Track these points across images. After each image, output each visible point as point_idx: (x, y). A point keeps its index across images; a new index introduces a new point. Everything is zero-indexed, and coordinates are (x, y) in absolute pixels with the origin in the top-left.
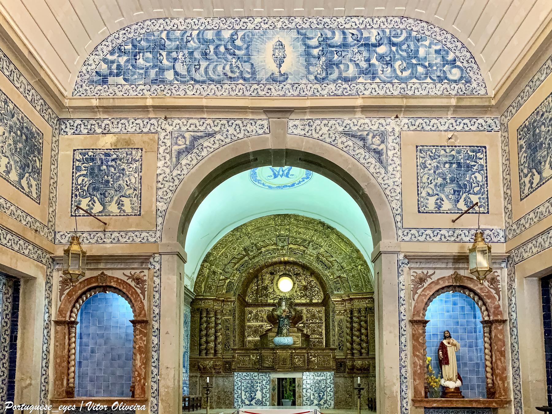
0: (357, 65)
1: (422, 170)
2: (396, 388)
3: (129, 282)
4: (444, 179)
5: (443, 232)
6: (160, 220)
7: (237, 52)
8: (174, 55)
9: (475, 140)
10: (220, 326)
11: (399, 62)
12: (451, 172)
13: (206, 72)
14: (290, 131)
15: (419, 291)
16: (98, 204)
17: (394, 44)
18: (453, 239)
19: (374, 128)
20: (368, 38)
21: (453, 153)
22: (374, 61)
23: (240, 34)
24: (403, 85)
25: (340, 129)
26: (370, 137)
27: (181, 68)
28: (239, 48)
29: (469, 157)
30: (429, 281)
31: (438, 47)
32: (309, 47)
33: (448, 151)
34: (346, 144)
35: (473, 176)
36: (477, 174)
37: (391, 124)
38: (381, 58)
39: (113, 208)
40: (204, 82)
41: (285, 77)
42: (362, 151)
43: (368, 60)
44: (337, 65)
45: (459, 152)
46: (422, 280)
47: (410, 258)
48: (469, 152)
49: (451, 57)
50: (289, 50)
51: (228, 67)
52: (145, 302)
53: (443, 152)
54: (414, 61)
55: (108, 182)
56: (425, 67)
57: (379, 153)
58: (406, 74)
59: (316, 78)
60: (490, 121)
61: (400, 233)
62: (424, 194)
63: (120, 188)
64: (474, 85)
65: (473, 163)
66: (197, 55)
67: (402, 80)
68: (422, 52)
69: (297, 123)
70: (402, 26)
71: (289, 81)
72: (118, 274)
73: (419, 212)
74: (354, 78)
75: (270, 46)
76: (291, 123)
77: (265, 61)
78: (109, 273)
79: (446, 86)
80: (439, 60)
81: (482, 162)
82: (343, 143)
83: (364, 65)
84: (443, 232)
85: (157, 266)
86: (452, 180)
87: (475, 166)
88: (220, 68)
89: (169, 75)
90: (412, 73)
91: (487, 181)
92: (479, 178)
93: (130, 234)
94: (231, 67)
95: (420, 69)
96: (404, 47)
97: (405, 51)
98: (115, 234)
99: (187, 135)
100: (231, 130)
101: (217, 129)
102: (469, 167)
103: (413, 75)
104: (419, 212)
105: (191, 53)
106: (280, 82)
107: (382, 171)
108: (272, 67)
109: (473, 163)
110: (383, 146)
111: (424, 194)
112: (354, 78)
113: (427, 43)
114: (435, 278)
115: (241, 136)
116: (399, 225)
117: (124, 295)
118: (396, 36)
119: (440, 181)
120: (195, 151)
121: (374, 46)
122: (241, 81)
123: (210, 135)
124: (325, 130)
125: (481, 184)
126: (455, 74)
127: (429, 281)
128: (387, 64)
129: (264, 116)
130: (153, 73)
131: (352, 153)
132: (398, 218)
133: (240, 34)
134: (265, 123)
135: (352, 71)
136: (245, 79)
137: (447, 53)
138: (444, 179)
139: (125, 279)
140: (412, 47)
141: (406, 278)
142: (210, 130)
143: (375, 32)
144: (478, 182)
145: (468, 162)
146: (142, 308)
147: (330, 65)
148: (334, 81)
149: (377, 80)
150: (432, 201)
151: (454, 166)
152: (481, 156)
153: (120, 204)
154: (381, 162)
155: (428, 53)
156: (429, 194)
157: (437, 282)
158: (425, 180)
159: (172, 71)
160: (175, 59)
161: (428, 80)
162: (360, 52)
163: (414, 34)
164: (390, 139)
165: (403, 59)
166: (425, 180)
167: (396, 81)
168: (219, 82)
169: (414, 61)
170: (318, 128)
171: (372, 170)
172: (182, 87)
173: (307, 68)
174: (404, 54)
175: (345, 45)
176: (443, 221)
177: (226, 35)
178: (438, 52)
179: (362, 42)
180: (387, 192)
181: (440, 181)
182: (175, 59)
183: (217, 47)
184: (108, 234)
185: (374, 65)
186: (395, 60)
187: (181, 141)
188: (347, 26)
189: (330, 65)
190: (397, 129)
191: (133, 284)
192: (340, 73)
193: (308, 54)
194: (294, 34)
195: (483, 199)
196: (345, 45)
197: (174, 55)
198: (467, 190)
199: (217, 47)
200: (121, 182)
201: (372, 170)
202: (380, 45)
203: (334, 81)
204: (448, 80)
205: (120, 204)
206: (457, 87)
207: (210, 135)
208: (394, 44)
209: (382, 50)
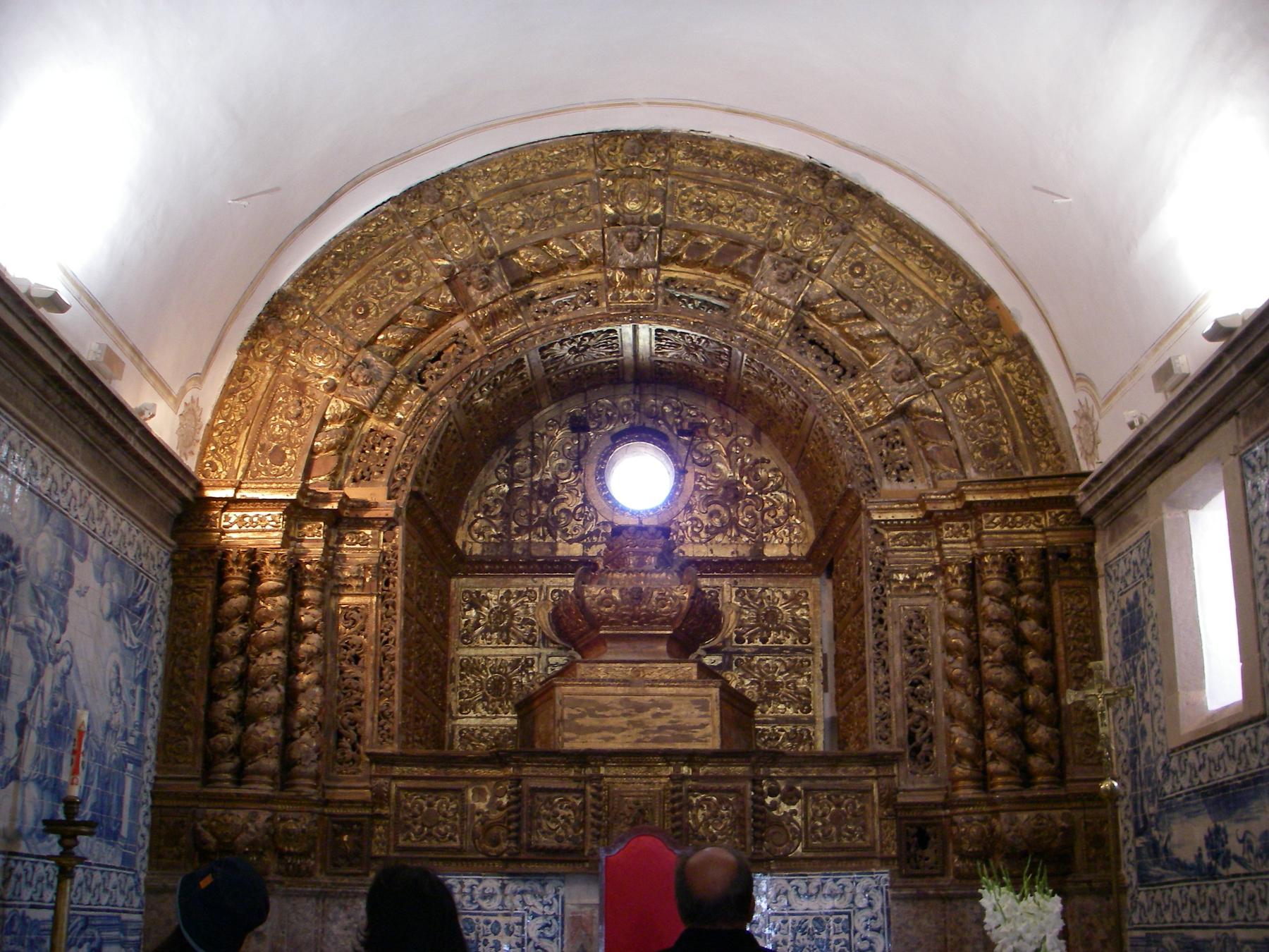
10: (312, 642)
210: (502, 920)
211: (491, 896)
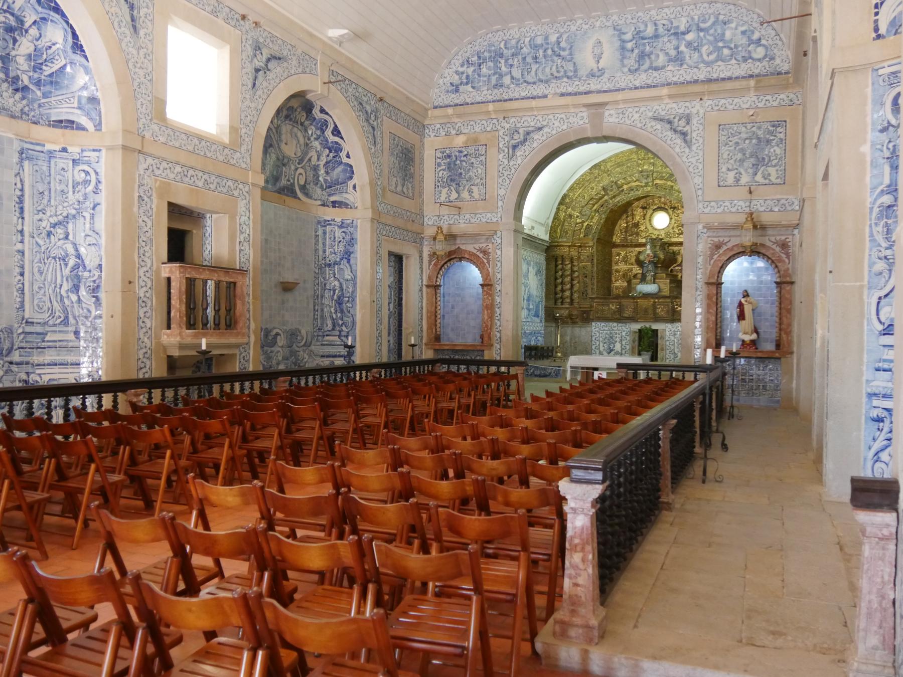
0: (667, 54)
3: (478, 253)
4: (744, 154)
6: (500, 203)
7: (562, 53)
8: (510, 62)
9: (774, 116)
11: (706, 47)
13: (536, 74)
14: (606, 120)
15: (715, 257)
16: (454, 192)
17: (702, 30)
19: (681, 111)
20: (677, 27)
22: (682, 48)
23: (565, 37)
24: (709, 69)
25: (650, 114)
26: (676, 120)
27: (516, 73)
28: (564, 50)
30: (725, 248)
31: (744, 28)
32: (624, 41)
36: (776, 148)
37: (696, 107)
38: (689, 44)
39: (465, 195)
40: (534, 83)
41: (602, 71)
42: (669, 133)
43: (677, 48)
44: (649, 56)
47: (709, 228)
49: (756, 36)
50: (606, 47)
51: (554, 68)
52: (490, 270)
53: (744, 129)
54: (721, 44)
55: (461, 174)
56: (731, 49)
57: (684, 134)
58: (712, 57)
59: (629, 70)
60: (792, 96)
61: (701, 205)
62: (724, 169)
64: (778, 61)
66: (529, 60)
67: (708, 64)
68: (728, 35)
69: (612, 112)
70: (710, 11)
71: (606, 75)
72: (470, 248)
74: (663, 67)
75: (590, 43)
76: (607, 113)
77: (586, 59)
78: (463, 247)
79: (750, 65)
80: (744, 41)
81: (782, 136)
82: (652, 127)
83: (673, 53)
85: (499, 241)
86: (751, 156)
88: (547, 70)
89: (507, 80)
90: (718, 56)
92: (778, 151)
93: (478, 215)
94: (557, 68)
95: (726, 52)
96: (712, 31)
97: (712, 35)
98: (467, 216)
99: (521, 131)
100: (557, 124)
101: (545, 123)
102: (768, 142)
103: (720, 58)
105: (524, 59)
106: (598, 77)
107: (687, 150)
108: (591, 64)
110: (687, 128)
111: (724, 169)
112: (663, 67)
113: (733, 25)
114: (730, 245)
115: (565, 127)
116: (700, 198)
117: (474, 264)
118: (704, 21)
119: (740, 156)
120: (527, 143)
121: (684, 33)
122: (565, 79)
123: (540, 129)
124: (636, 116)
126: (760, 52)
127: (725, 248)
128: (695, 50)
129: (584, 109)
130: (494, 79)
131: (660, 135)
132: (700, 193)
133: (565, 37)
134: (585, 114)
135: (662, 60)
136: (568, 78)
137: (753, 32)
138: (744, 154)
139: (475, 251)
140: (719, 31)
141: (702, 247)
142: (539, 125)
143: (684, 20)
146: (488, 274)
147: (642, 56)
148: (646, 71)
149: (685, 66)
150: (731, 175)
151: (754, 141)
154: (685, 141)
155: (734, 35)
156: (728, 170)
157: (731, 249)
158: (725, 156)
159: (509, 77)
160: (511, 66)
161: (733, 61)
162: (669, 41)
163: (721, 17)
164: (694, 121)
165: (710, 43)
166: (725, 156)
167: (702, 65)
168: (547, 82)
169: (721, 44)
170: (630, 115)
171: (677, 150)
172: (517, 89)
173: (622, 61)
174: (711, 38)
175: (656, 36)
177: (553, 38)
178: (743, 33)
179: (672, 31)
180: (691, 169)
181: (740, 156)
182: (511, 66)
183: (545, 51)
184: (462, 216)
185: (682, 52)
186: (702, 46)
187: (516, 136)
188: (659, 17)
189: (642, 56)
190: (702, 111)
191: (481, 255)
192: (651, 63)
193: (623, 48)
194: (611, 31)
196: (656, 36)
197: (510, 62)
199: (545, 51)
200: (471, 173)
202: (688, 32)
203: (646, 71)
204: (753, 59)
206: (761, 65)
207: (540, 129)
208: (702, 30)
209: (690, 37)
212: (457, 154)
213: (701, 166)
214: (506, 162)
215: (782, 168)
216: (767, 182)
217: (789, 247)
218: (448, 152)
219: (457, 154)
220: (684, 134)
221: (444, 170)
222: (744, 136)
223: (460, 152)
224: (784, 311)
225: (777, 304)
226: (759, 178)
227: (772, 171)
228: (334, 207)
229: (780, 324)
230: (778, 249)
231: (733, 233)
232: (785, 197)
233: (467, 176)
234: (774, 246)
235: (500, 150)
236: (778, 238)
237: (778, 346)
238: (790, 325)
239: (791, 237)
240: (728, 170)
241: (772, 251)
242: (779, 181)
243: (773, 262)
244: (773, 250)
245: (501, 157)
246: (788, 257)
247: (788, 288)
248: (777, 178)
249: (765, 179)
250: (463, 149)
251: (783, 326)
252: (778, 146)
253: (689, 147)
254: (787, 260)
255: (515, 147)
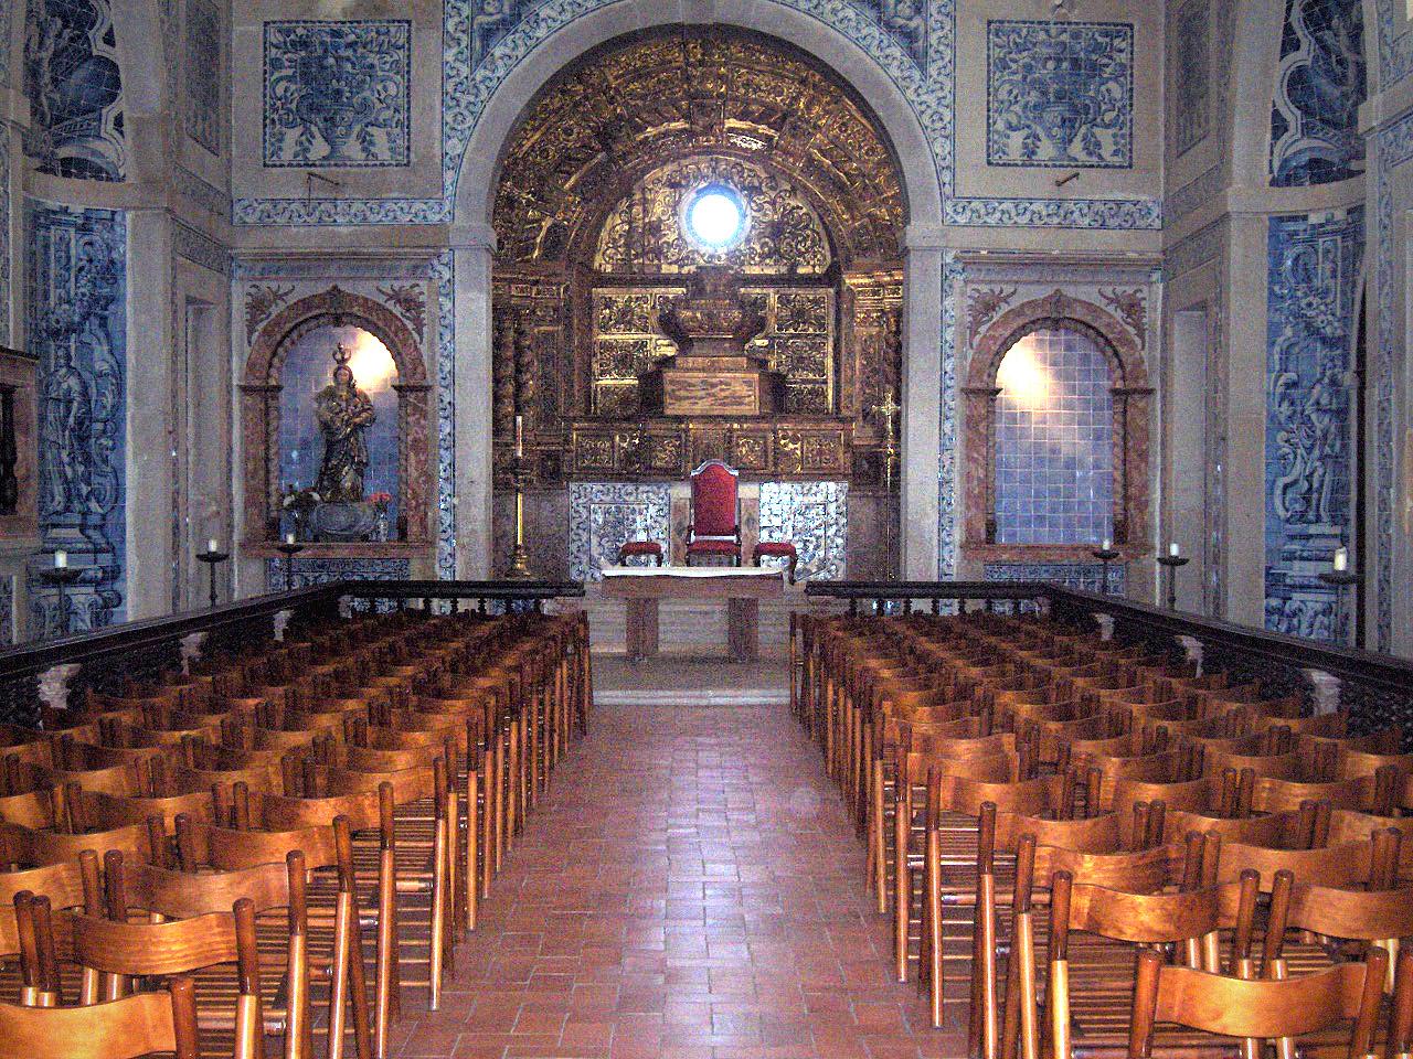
1: (998, 75)
2: (932, 519)
3: (390, 305)
4: (1044, 93)
5: (1036, 207)
6: (449, 176)
12: (1058, 78)
15: (983, 329)
18: (1056, 220)
21: (1065, 37)
29: (1097, 48)
30: (1005, 308)
33: (1053, 32)
34: (841, 15)
35: (1103, 88)
36: (1112, 85)
39: (352, 149)
42: (875, 31)
45: (1076, 36)
46: (990, 307)
48: (1096, 35)
52: (424, 348)
53: (1042, 36)
55: (339, 92)
62: (1000, 126)
63: (365, 106)
65: (1106, 61)
72: (365, 289)
73: (989, 163)
81: (1123, 58)
82: (834, 12)
84: (1036, 207)
85: (447, 275)
86: (1060, 97)
87: (1107, 66)
91: (1131, 97)
92: (1117, 91)
93: (389, 205)
98: (357, 206)
102: (1095, 69)
104: (989, 163)
107: (917, 74)
109: (1106, 61)
111: (1000, 126)
114: (1015, 303)
116: (948, 190)
119: (1034, 97)
120: (521, 27)
125: (1119, 104)
127: (1005, 308)
131: (854, 34)
138: (1044, 93)
139: (381, 300)
141: (956, 305)
144: (1112, 101)
145: (1094, 57)
146: (418, 360)
150: (1016, 140)
151: (1065, 65)
152: (1123, 45)
153: (366, 141)
154: (913, 54)
156: (1010, 127)
157: (1018, 312)
158: (1003, 95)
166: (1003, 95)
176: (1037, 183)
180: (926, 120)
181: (1034, 97)
184: (341, 205)
191: (397, 310)
195: (1123, 136)
198: (1090, 116)
200: (367, 94)
201: (896, 73)
205: (366, 141)
210: (636, 507)
211: (631, 494)
212: (328, 39)
213: (947, 115)
214: (465, 70)
215: (1126, 131)
216: (1094, 160)
217: (1143, 310)
218: (300, 31)
219: (328, 39)
220: (909, 36)
221: (290, 79)
222: (1046, 51)
223: (336, 34)
224: (1133, 455)
225: (1117, 439)
226: (1076, 148)
227: (1105, 136)
228: (67, 174)
229: (1125, 487)
230: (1119, 315)
231: (1027, 275)
232: (1132, 197)
233: (356, 100)
234: (1111, 309)
235: (448, 40)
236: (1119, 290)
237: (1120, 533)
238: (1145, 487)
239: (1145, 288)
240: (1010, 127)
241: (1105, 319)
242: (1117, 160)
243: (1108, 342)
244: (1111, 316)
245: (450, 55)
246: (1141, 335)
247: (1141, 405)
248: (1116, 153)
249: (1090, 154)
250: (345, 28)
251: (1132, 491)
252: (1116, 79)
253: (923, 68)
254: (1138, 340)
255: (488, 34)
